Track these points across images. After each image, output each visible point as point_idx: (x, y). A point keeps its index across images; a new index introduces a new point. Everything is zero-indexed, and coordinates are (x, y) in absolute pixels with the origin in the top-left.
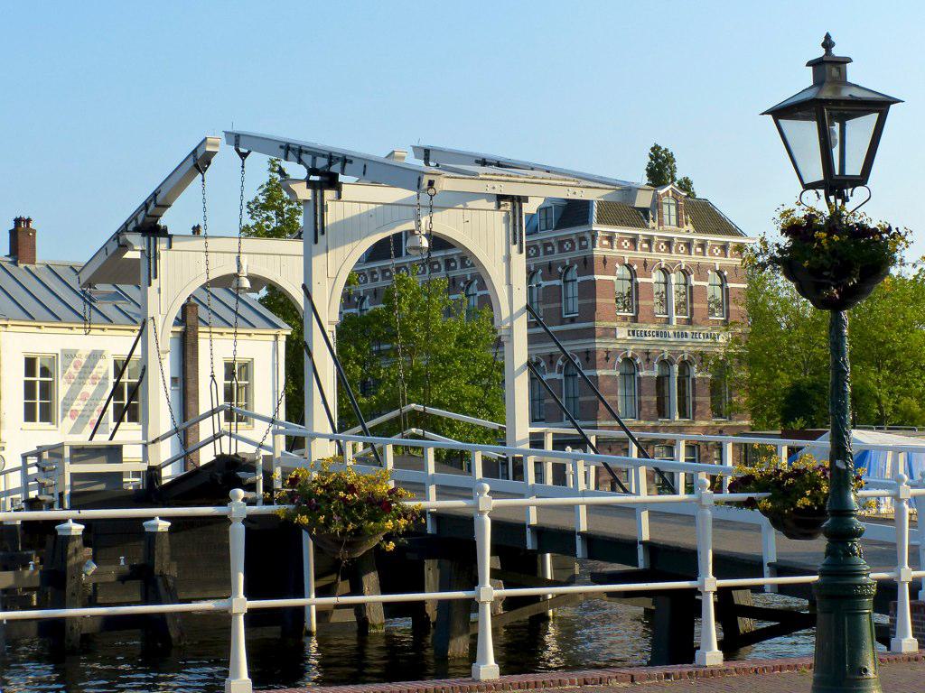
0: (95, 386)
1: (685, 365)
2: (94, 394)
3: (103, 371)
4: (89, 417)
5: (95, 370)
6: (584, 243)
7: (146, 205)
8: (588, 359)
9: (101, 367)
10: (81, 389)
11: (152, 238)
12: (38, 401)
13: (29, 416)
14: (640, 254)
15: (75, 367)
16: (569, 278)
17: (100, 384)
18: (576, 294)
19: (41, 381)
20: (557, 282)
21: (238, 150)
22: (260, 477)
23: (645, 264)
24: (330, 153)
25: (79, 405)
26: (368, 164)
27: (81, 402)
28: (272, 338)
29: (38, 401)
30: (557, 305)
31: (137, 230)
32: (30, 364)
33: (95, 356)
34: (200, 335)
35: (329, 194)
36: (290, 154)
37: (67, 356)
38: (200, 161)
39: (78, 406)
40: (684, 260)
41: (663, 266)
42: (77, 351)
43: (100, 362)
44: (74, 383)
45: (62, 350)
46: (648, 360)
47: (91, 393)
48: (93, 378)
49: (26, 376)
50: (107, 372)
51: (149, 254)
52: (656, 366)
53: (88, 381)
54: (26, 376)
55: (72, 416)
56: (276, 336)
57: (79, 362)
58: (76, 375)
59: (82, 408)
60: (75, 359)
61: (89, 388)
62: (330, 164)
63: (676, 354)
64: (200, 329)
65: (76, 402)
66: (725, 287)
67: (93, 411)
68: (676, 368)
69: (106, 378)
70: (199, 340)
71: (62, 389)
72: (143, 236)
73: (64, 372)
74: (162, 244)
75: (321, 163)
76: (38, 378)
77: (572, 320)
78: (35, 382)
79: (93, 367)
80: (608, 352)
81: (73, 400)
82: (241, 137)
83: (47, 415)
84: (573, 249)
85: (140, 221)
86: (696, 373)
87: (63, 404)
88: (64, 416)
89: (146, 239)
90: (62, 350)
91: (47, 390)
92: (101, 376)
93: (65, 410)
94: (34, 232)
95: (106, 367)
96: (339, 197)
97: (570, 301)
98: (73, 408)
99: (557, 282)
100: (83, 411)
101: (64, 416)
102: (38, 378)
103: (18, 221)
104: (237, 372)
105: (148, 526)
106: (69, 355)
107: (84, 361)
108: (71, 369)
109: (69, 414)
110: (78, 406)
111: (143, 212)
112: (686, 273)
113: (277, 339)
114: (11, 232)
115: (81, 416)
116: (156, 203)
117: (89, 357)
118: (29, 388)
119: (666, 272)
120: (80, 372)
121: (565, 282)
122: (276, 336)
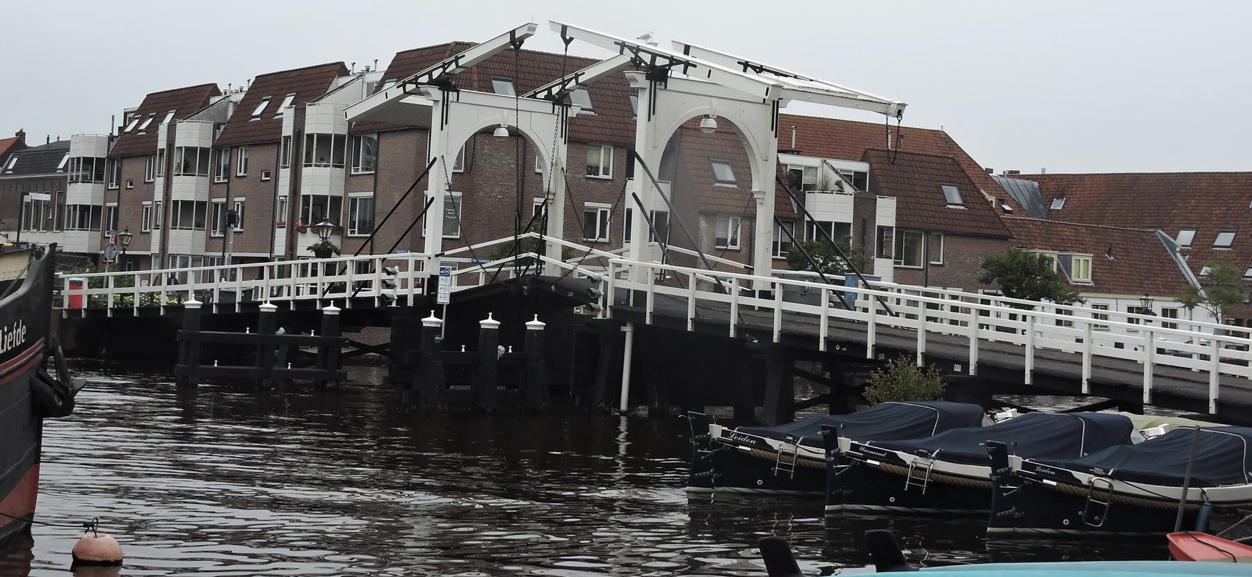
11: (446, 92)
21: (563, 35)
24: (672, 57)
31: (432, 82)
62: (671, 64)
75: (660, 62)
82: (568, 28)
85: (435, 76)
96: (666, 87)
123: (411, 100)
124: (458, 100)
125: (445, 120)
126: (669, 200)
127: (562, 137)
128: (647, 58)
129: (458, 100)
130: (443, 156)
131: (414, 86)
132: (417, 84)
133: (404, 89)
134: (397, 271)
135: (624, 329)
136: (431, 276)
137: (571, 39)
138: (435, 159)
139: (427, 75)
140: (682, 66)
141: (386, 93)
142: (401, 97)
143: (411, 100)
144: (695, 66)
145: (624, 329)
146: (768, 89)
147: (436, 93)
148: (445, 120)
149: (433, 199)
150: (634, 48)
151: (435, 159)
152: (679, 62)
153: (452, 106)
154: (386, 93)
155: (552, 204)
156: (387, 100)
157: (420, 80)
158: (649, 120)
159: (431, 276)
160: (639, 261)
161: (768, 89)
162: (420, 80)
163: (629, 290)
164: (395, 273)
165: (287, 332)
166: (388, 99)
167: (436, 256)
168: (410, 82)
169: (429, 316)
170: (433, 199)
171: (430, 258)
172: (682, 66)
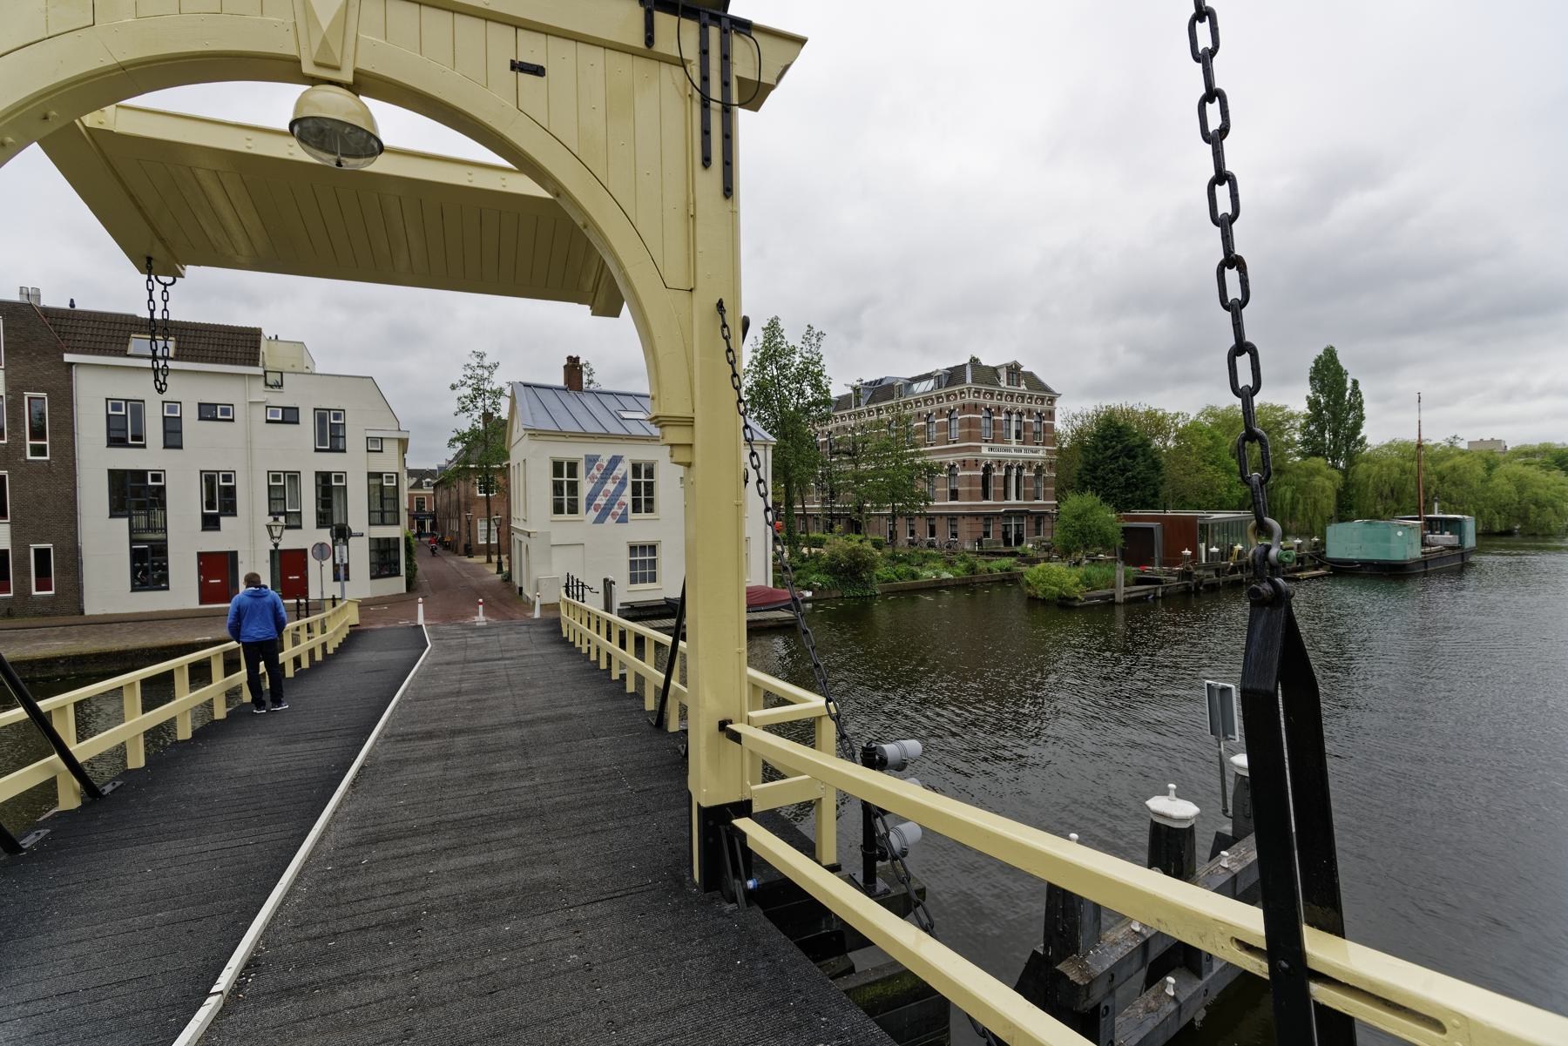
0: (615, 485)
1: (1020, 468)
2: (615, 491)
3: (623, 472)
4: (611, 509)
5: (615, 473)
6: (963, 395)
8: (964, 465)
9: (620, 469)
14: (995, 402)
15: (598, 469)
16: (952, 417)
18: (957, 426)
23: (999, 408)
25: (602, 500)
27: (604, 498)
28: (763, 447)
30: (945, 433)
32: (557, 467)
33: (615, 461)
37: (590, 461)
39: (601, 500)
40: (1020, 407)
42: (599, 456)
44: (597, 483)
45: (586, 456)
46: (999, 466)
47: (612, 491)
48: (613, 478)
49: (554, 477)
50: (626, 473)
53: (610, 480)
54: (554, 477)
55: (596, 510)
56: (765, 446)
57: (602, 466)
58: (598, 476)
60: (598, 463)
61: (610, 486)
63: (1015, 462)
65: (599, 498)
67: (614, 504)
68: (1015, 469)
69: (625, 478)
71: (585, 487)
73: (588, 472)
77: (954, 442)
78: (563, 481)
79: (614, 469)
80: (976, 461)
81: (596, 496)
83: (573, 509)
84: (956, 399)
86: (1025, 473)
87: (588, 499)
88: (588, 509)
90: (586, 456)
91: (573, 487)
92: (620, 477)
95: (624, 468)
97: (953, 431)
98: (596, 502)
100: (606, 504)
101: (588, 509)
103: (570, 358)
106: (592, 460)
107: (605, 464)
108: (594, 471)
109: (592, 507)
110: (601, 500)
112: (1020, 414)
115: (604, 509)
117: (610, 462)
118: (557, 488)
119: (1009, 413)
120: (602, 474)
121: (950, 420)
122: (765, 446)
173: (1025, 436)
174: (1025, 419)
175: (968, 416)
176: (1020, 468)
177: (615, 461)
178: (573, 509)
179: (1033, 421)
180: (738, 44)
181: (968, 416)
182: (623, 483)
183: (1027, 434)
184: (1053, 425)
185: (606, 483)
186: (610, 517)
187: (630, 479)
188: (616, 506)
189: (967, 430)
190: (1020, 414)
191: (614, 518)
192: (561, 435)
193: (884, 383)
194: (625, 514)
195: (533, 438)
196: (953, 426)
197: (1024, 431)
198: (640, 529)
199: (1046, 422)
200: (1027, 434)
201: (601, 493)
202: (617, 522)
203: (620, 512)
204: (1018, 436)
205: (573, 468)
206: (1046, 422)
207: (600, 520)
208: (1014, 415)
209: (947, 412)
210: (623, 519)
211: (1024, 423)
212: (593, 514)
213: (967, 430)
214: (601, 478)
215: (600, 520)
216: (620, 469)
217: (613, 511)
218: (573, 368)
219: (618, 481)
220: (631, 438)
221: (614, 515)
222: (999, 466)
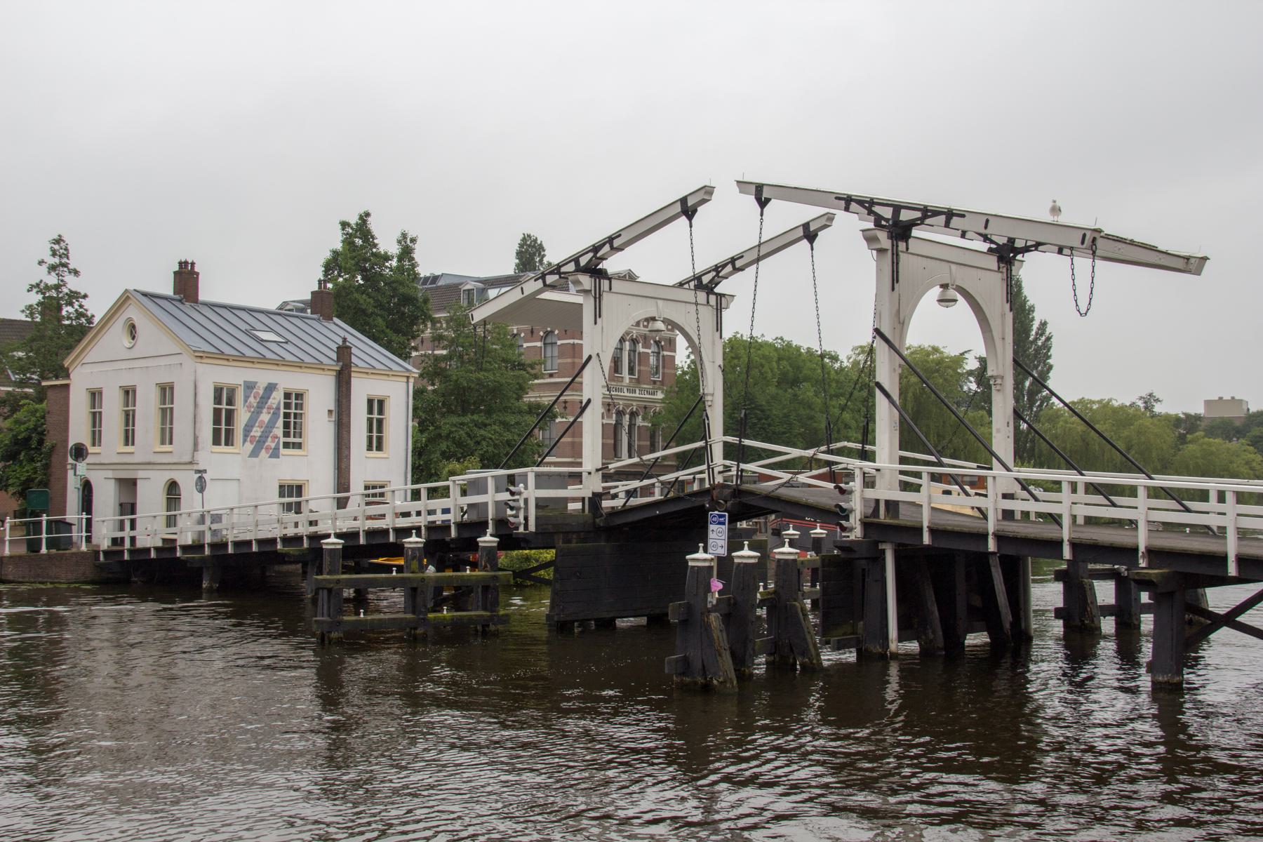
1: (633, 415)
2: (269, 422)
3: (276, 402)
4: (264, 442)
5: (270, 401)
7: (596, 249)
9: (274, 398)
10: (258, 417)
12: (223, 427)
13: (216, 442)
15: (255, 397)
16: (549, 340)
17: (273, 413)
19: (226, 409)
20: (539, 344)
21: (758, 199)
22: (522, 505)
24: (926, 207)
25: (257, 431)
26: (990, 218)
27: (258, 429)
28: (405, 379)
29: (223, 427)
31: (579, 269)
32: (218, 392)
33: (271, 388)
34: (353, 374)
35: (902, 245)
36: (854, 206)
38: (688, 210)
39: (257, 432)
41: (634, 337)
42: (256, 383)
43: (274, 394)
44: (253, 412)
45: (245, 382)
46: (609, 410)
48: (269, 408)
49: (215, 404)
51: (595, 294)
52: (614, 415)
54: (215, 404)
56: (408, 377)
57: (258, 393)
58: (255, 405)
59: (258, 434)
60: (255, 390)
61: (265, 417)
63: (628, 406)
64: (353, 369)
65: (255, 429)
66: (661, 354)
68: (627, 416)
69: (278, 408)
70: (352, 379)
71: (242, 417)
72: (591, 277)
73: (246, 401)
74: (605, 283)
75: (905, 216)
76: (224, 406)
77: (551, 376)
79: (269, 398)
81: (252, 427)
82: (765, 188)
83: (229, 442)
86: (639, 421)
88: (245, 441)
89: (593, 280)
90: (245, 382)
91: (230, 415)
92: (274, 406)
93: (246, 436)
94: (197, 274)
95: (277, 398)
96: (907, 249)
98: (252, 434)
99: (539, 344)
101: (245, 441)
102: (224, 406)
104: (376, 406)
105: (327, 544)
106: (250, 386)
107: (261, 392)
108: (251, 399)
109: (249, 439)
110: (257, 432)
111: (591, 255)
113: (408, 382)
114: (175, 273)
115: (259, 441)
116: (612, 243)
117: (266, 389)
118: (217, 413)
120: (258, 402)
121: (545, 344)
122: (408, 377)
123: (548, 295)
124: (610, 289)
125: (598, 313)
126: (878, 392)
127: (717, 330)
128: (887, 213)
129: (610, 289)
130: (598, 355)
131: (557, 277)
132: (559, 273)
133: (544, 282)
134: (522, 490)
135: (881, 546)
136: (593, 493)
137: (768, 200)
138: (590, 358)
139: (573, 263)
140: (942, 218)
141: (522, 288)
142: (540, 291)
143: (548, 295)
144: (963, 216)
145: (881, 546)
146: (1084, 236)
147: (586, 281)
148: (598, 313)
149: (589, 401)
150: (866, 202)
151: (590, 358)
152: (936, 213)
153: (605, 297)
154: (522, 288)
155: (710, 406)
156: (522, 296)
157: (563, 269)
158: (893, 289)
159: (593, 493)
160: (900, 464)
161: (1084, 236)
162: (563, 269)
163: (877, 501)
164: (520, 493)
165: (438, 570)
166: (525, 295)
167: (598, 470)
168: (551, 273)
169: (742, 549)
170: (589, 401)
171: (590, 473)
172: (942, 218)
173: (639, 371)
174: (640, 348)
175: (571, 341)
176: (633, 415)
177: (271, 388)
178: (229, 442)
179: (649, 351)
180: (723, 299)
181: (571, 341)
182: (275, 415)
183: (642, 368)
184: (674, 357)
185: (261, 413)
186: (263, 450)
187: (282, 410)
188: (270, 439)
189: (569, 360)
190: (634, 342)
191: (267, 453)
192: (220, 356)
193: (441, 283)
194: (277, 448)
195: (199, 360)
196: (549, 354)
197: (639, 365)
198: (289, 467)
199: (665, 353)
200: (642, 368)
201: (257, 424)
202: (270, 457)
203: (273, 445)
204: (631, 371)
205: (232, 392)
206: (665, 353)
207: (254, 454)
208: (627, 343)
209: (541, 334)
210: (275, 454)
211: (639, 353)
212: (249, 447)
213: (569, 360)
214: (258, 407)
215: (254, 454)
216: (274, 398)
217: (267, 444)
218: (186, 278)
219: (272, 411)
220: (263, 360)
221: (267, 449)
222: (609, 410)
